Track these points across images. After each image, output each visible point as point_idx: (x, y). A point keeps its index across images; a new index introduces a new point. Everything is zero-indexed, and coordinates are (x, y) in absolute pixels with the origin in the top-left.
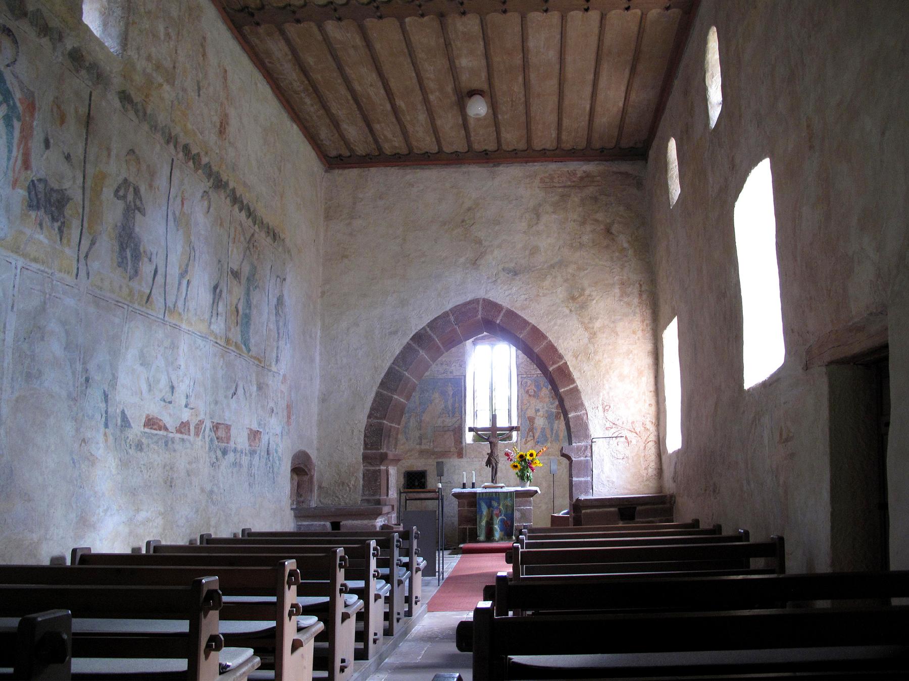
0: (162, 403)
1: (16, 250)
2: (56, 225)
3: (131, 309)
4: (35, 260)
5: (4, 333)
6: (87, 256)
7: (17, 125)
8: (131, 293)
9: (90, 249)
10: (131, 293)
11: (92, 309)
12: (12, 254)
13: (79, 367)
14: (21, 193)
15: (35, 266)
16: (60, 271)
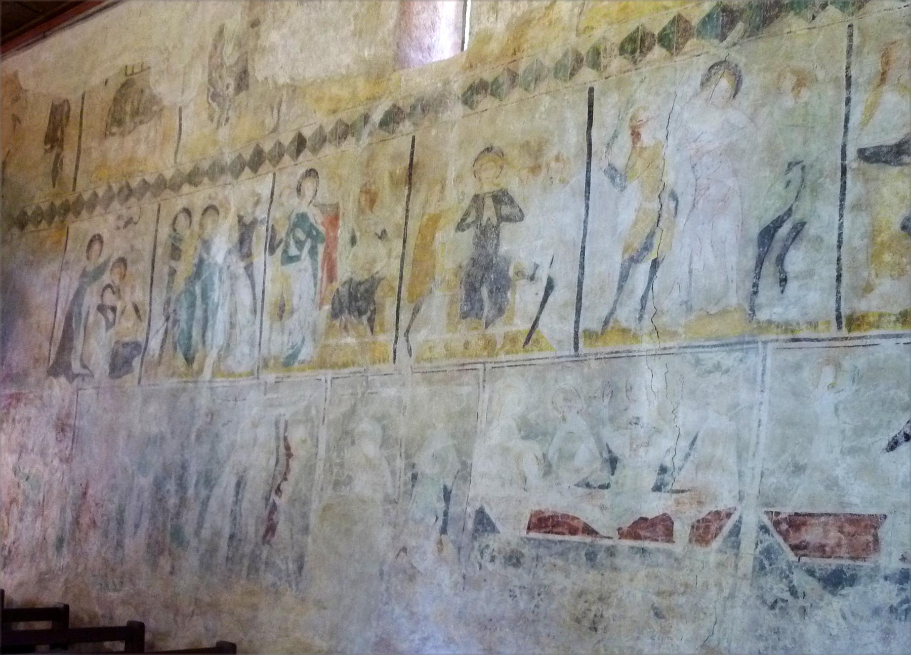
0: (581, 491)
1: (322, 364)
2: (364, 318)
3: (489, 366)
4: (345, 365)
5: (317, 446)
6: (408, 331)
7: (321, 248)
8: (490, 345)
9: (412, 320)
10: (490, 345)
11: (423, 390)
12: (320, 371)
13: (400, 463)
14: (327, 307)
15: (346, 371)
16: (374, 363)
